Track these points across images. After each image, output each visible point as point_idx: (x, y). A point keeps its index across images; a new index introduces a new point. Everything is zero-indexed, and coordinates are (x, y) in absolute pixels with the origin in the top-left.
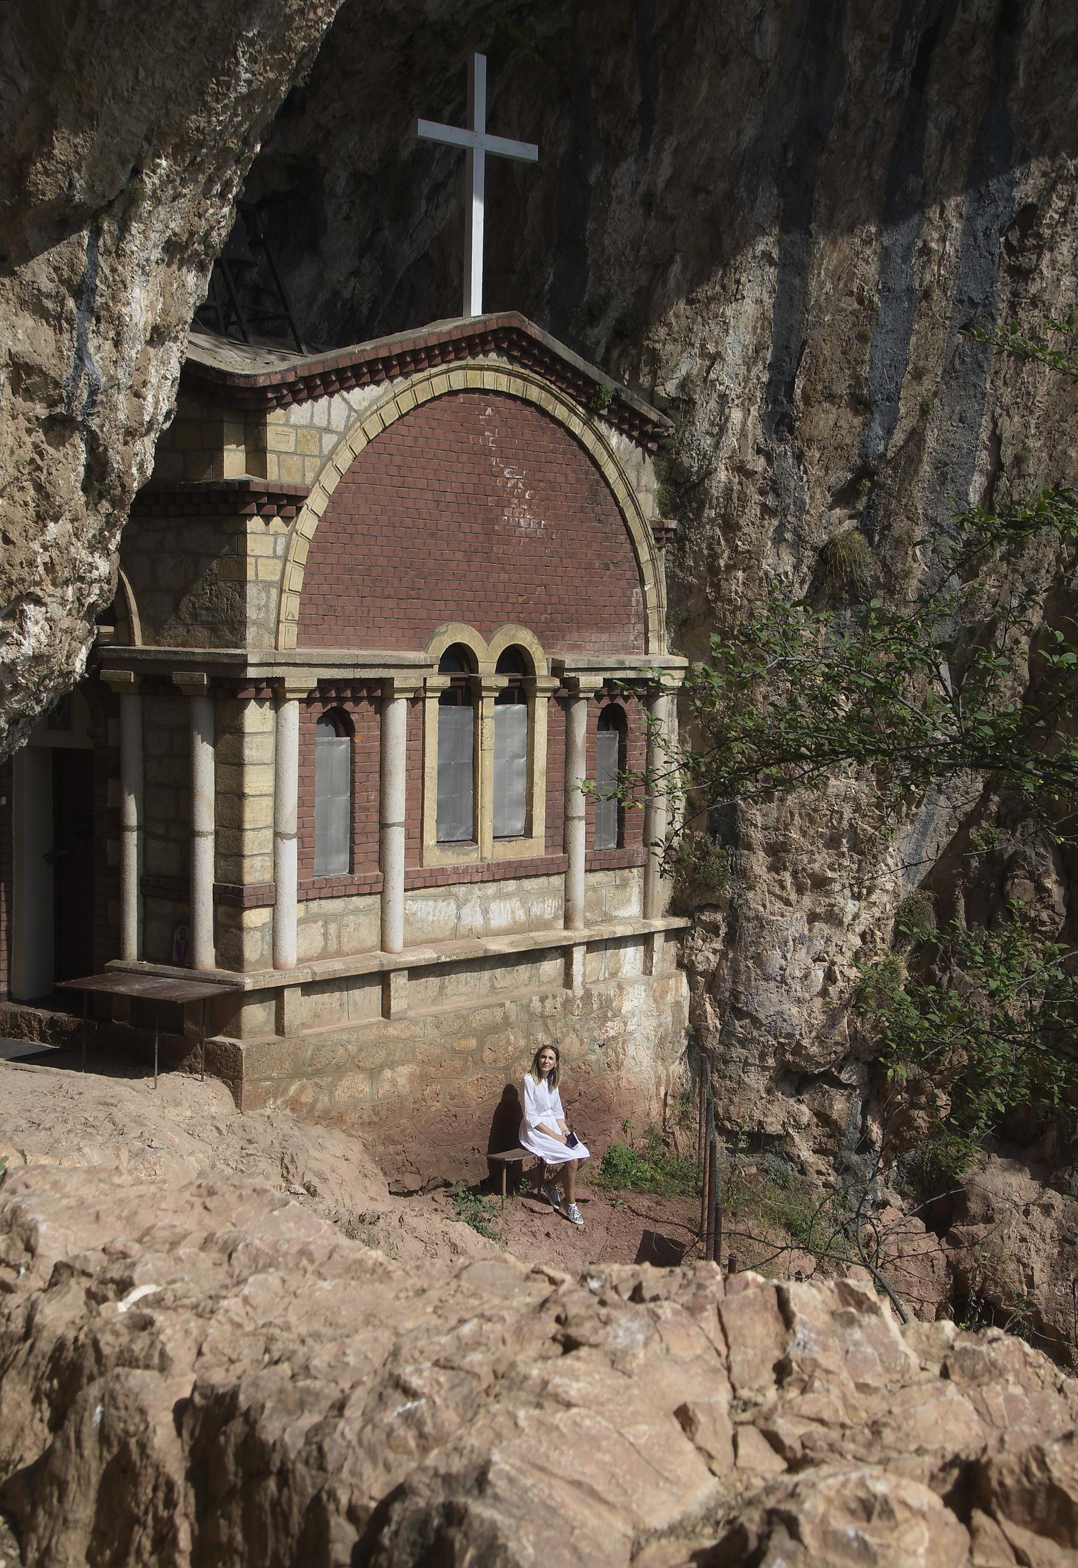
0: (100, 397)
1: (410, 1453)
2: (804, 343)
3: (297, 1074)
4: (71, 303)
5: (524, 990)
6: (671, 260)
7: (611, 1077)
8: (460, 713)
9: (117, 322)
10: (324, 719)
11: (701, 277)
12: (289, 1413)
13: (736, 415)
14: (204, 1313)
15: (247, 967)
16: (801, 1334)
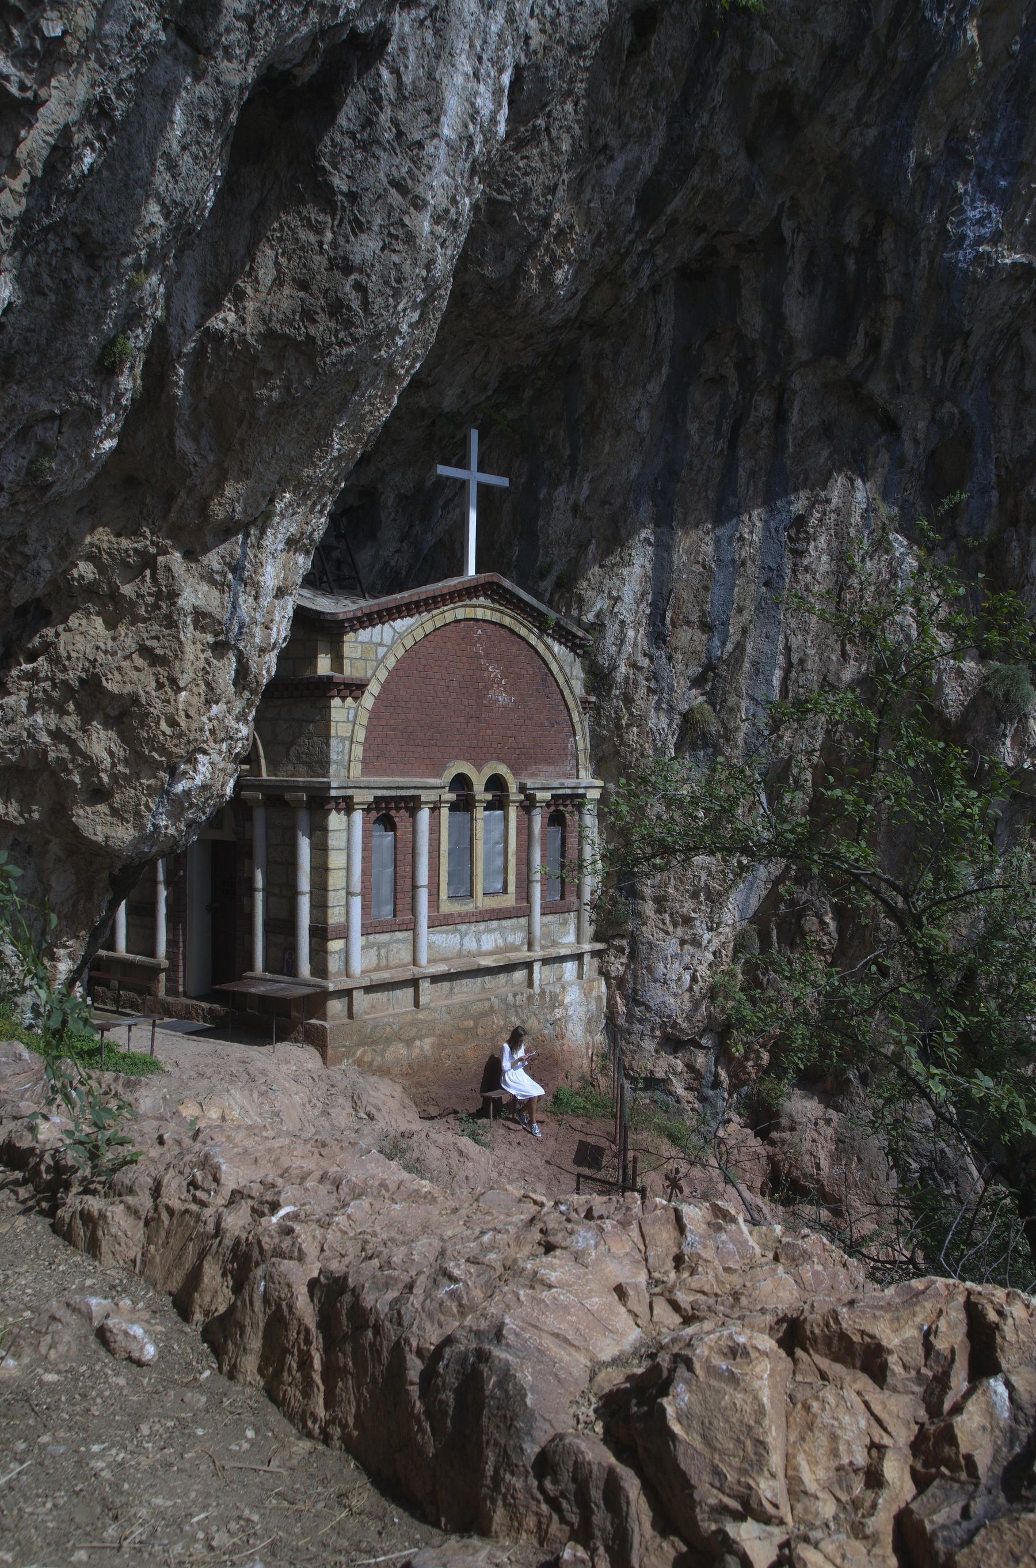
0: (245, 630)
1: (454, 1316)
2: (671, 591)
3: (361, 1043)
4: (230, 576)
5: (503, 990)
6: (589, 542)
7: (558, 1044)
8: (462, 816)
9: (257, 586)
10: (378, 821)
11: (608, 552)
12: (379, 1290)
13: (631, 633)
14: (324, 1224)
15: (330, 976)
16: (690, 1238)
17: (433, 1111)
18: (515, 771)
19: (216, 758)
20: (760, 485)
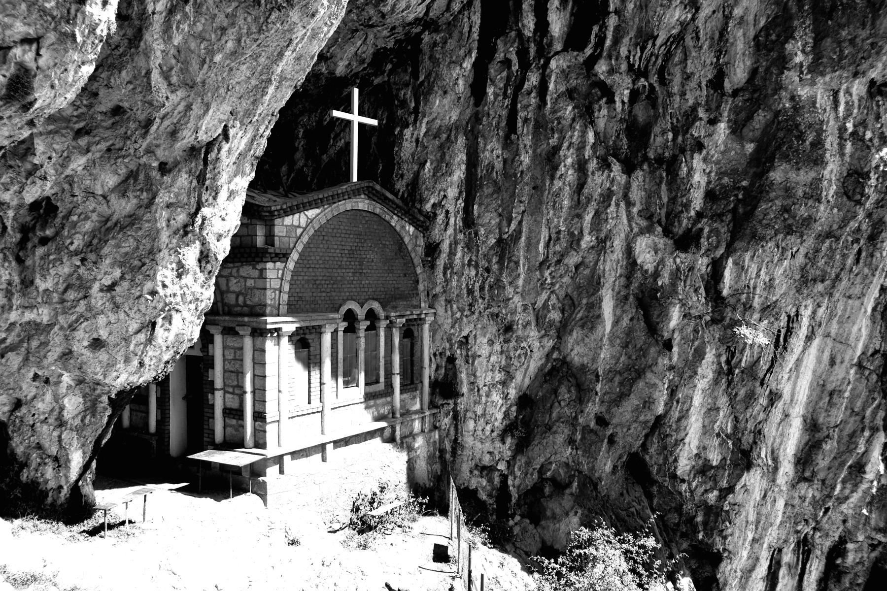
6: (426, 162)
17: (336, 526)
18: (384, 307)
20: (531, 126)
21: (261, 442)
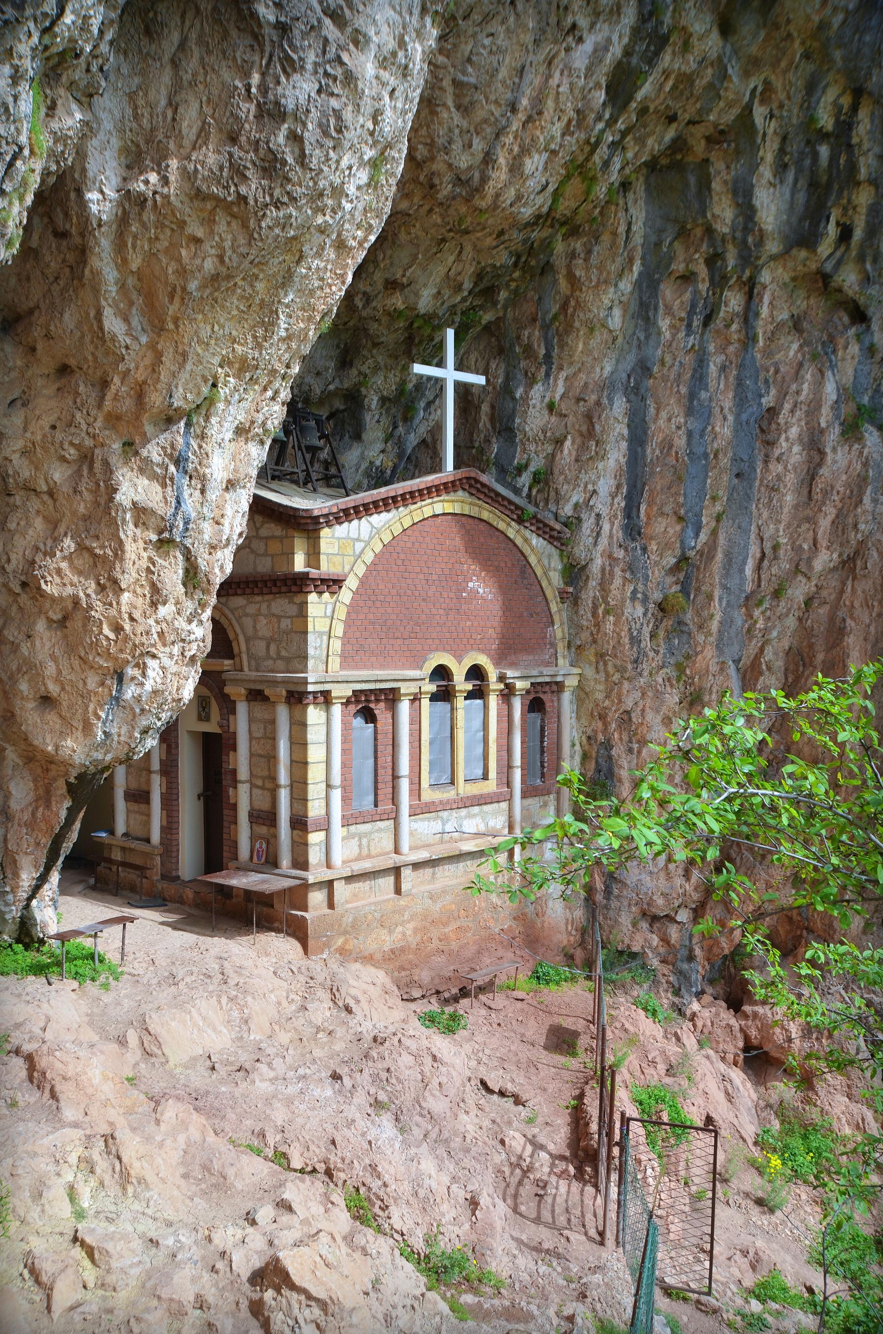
0: (191, 526)
2: (644, 484)
4: (172, 468)
8: (443, 707)
9: (203, 479)
13: (606, 527)
19: (166, 661)
20: (731, 379)
21: (301, 859)
